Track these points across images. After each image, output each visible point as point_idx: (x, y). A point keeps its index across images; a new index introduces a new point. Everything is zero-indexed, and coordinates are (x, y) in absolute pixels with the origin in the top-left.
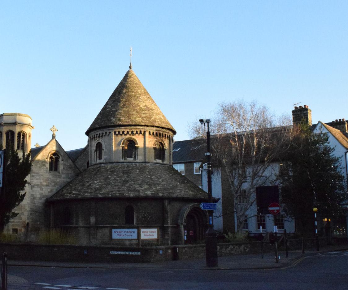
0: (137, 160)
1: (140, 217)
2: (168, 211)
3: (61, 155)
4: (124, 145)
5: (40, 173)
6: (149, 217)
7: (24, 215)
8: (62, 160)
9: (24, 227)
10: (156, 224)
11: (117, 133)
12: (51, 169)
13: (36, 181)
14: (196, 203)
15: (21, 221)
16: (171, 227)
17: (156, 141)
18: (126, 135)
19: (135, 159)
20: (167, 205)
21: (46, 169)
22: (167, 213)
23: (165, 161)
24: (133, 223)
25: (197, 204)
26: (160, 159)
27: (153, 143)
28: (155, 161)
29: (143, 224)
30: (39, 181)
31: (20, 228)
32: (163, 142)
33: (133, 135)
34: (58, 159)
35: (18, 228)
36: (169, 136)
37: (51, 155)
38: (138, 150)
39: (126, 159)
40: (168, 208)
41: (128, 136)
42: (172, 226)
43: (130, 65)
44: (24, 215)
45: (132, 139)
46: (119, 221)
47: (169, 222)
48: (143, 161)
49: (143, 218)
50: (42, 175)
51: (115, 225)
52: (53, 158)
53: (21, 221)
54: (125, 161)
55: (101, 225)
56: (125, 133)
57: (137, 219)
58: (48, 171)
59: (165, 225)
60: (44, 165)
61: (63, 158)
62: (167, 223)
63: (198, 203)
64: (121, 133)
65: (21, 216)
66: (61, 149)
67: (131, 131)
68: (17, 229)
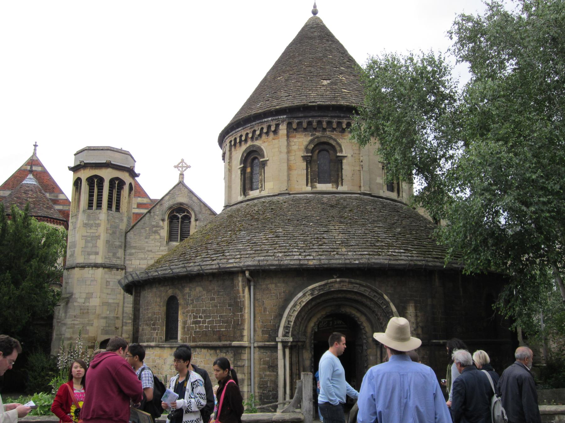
0: (264, 193)
1: (189, 322)
2: (244, 305)
3: (193, 210)
4: (242, 166)
5: (146, 249)
6: (204, 322)
7: (92, 325)
8: (196, 220)
10: (220, 340)
11: (233, 143)
12: (171, 237)
13: (137, 262)
14: (338, 280)
16: (260, 347)
17: (311, 142)
18: (246, 141)
19: (262, 190)
20: (241, 289)
21: (160, 239)
22: (241, 309)
23: (342, 185)
24: (177, 338)
25: (340, 282)
26: (330, 183)
27: (303, 147)
28: (309, 189)
29: (194, 341)
30: (145, 261)
32: (335, 140)
33: (257, 139)
34: (190, 218)
37: (172, 212)
38: (266, 168)
39: (249, 195)
40: (244, 297)
41: (250, 143)
42: (261, 344)
43: (315, 6)
44: (92, 325)
45: (254, 149)
46: (157, 335)
47: (245, 333)
48: (277, 192)
49: (194, 325)
50: (151, 251)
51: (153, 344)
52: (178, 218)
56: (243, 138)
57: (184, 328)
58: (165, 243)
59: (235, 343)
60: (156, 232)
61: (200, 216)
62: (241, 338)
63: (347, 280)
64: (238, 140)
65: (88, 328)
66: (194, 198)
67: (253, 130)
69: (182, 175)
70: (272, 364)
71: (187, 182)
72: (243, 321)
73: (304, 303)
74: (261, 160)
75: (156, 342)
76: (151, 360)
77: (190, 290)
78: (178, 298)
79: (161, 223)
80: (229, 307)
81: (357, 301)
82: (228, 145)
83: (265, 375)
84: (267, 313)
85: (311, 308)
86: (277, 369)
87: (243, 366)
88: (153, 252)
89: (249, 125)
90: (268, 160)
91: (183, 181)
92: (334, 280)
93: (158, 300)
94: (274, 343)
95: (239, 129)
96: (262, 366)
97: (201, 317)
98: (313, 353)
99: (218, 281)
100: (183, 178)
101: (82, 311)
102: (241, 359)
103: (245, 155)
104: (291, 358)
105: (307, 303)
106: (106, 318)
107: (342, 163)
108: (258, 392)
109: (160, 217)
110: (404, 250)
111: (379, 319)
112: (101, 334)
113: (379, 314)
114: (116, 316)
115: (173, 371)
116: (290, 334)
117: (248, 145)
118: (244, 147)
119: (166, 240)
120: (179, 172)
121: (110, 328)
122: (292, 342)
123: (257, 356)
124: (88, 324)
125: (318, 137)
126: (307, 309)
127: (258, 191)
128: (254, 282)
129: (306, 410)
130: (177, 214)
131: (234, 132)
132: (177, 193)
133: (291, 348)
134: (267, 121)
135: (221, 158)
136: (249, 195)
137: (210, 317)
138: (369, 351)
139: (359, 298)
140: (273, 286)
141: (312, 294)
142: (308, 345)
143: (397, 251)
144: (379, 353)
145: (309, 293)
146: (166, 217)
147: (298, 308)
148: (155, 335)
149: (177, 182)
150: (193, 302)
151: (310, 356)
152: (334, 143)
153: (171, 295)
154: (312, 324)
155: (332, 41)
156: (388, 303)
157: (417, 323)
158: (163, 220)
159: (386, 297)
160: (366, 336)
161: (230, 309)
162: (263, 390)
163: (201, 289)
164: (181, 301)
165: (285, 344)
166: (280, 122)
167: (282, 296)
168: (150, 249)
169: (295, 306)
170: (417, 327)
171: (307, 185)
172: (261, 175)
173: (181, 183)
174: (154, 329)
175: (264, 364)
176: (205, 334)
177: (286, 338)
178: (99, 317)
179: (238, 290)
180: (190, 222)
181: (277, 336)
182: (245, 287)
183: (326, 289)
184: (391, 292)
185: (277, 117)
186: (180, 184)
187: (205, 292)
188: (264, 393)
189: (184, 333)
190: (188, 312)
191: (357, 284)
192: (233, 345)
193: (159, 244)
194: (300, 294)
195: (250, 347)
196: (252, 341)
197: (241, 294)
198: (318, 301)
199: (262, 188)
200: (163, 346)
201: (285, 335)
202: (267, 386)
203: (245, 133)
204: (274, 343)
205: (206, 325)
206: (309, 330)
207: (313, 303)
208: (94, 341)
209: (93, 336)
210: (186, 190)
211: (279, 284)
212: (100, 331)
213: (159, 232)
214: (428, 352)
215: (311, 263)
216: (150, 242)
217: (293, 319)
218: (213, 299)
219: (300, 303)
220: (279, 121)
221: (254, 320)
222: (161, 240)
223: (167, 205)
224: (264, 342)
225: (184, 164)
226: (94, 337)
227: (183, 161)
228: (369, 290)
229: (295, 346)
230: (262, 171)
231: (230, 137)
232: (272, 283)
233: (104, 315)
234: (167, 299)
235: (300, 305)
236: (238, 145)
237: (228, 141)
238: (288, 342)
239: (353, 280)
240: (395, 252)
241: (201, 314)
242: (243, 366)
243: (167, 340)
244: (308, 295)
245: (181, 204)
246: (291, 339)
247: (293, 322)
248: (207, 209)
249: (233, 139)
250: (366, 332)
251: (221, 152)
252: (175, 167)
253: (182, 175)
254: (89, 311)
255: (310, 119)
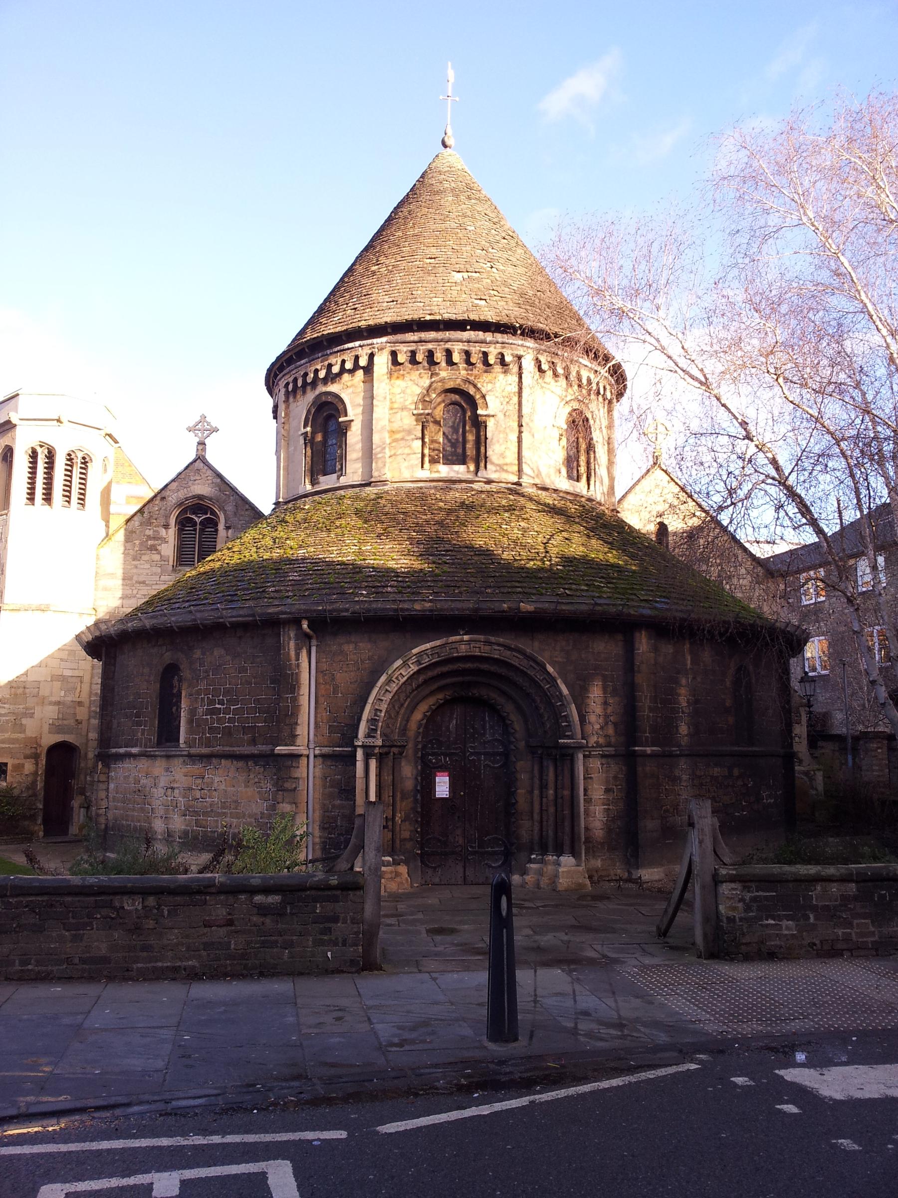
0: (343, 481)
1: (200, 710)
2: (298, 680)
7: (32, 716)
8: (228, 528)
9: (36, 757)
10: (254, 742)
11: (290, 387)
14: (466, 637)
15: (22, 736)
16: (323, 756)
19: (342, 475)
20: (293, 653)
22: (293, 686)
23: (486, 468)
28: (425, 474)
31: (16, 762)
32: (475, 386)
34: (216, 524)
35: (10, 762)
36: (508, 359)
37: (184, 511)
39: (318, 483)
40: (298, 666)
42: (326, 750)
44: (32, 716)
46: (143, 734)
49: (209, 717)
50: (144, 582)
51: (134, 750)
52: (195, 524)
53: (22, 736)
54: (318, 488)
55: (114, 750)
57: (190, 722)
58: (171, 568)
59: (280, 749)
60: (153, 548)
62: (292, 738)
63: (482, 637)
64: (300, 383)
65: (24, 721)
67: (326, 363)
68: (6, 764)
69: (202, 444)
70: (345, 786)
71: (210, 457)
72: (296, 708)
73: (405, 678)
74: (341, 420)
75: (141, 747)
76: (131, 780)
77: (203, 654)
78: (182, 667)
79: (163, 532)
80: (271, 684)
81: (500, 677)
82: (283, 391)
83: (334, 806)
84: (340, 695)
85: (418, 687)
86: (355, 796)
87: (295, 788)
88: (147, 585)
89: (320, 355)
90: (352, 421)
91: (204, 457)
92: (458, 637)
93: (146, 670)
94: (350, 749)
95: (303, 362)
96: (327, 790)
97: (221, 702)
98: (419, 767)
99: (253, 638)
100: (204, 450)
101: (13, 690)
102: (290, 778)
103: (313, 411)
104: (379, 775)
105: (411, 677)
106: (58, 703)
107: (486, 427)
108: (320, 837)
109: (162, 521)
110: (587, 585)
111: (537, 708)
112: (50, 733)
113: (538, 699)
114: (78, 700)
115: (170, 799)
116: (379, 732)
117: (317, 392)
118: (311, 396)
119: (171, 563)
120: (198, 440)
121: (65, 722)
122: (380, 747)
123: (318, 772)
124: (25, 715)
125: (442, 380)
126: (409, 688)
127: (335, 476)
128: (317, 638)
129: (370, 868)
130: (193, 516)
131: (293, 366)
132: (192, 478)
133: (381, 759)
134: (352, 348)
135: (272, 415)
136: (318, 483)
137: (236, 702)
138: (520, 765)
139: (503, 671)
140: (351, 647)
141: (418, 662)
142: (410, 750)
143: (574, 586)
144: (536, 768)
145: (414, 659)
146: (172, 521)
147: (394, 688)
148: (139, 734)
149: (193, 456)
150: (209, 676)
151: (415, 772)
152: (472, 391)
153: (169, 662)
154: (418, 716)
155: (478, 199)
156: (554, 680)
157: (606, 716)
158: (166, 526)
159: (550, 669)
160: (514, 738)
161: (275, 687)
162: (330, 833)
163: (223, 652)
164: (186, 673)
165: (369, 751)
166: (376, 350)
167: (367, 666)
168: (141, 579)
169: (389, 681)
170: (606, 724)
171: (422, 467)
172: (341, 447)
173: (200, 458)
174: (139, 724)
175: (331, 786)
176: (228, 732)
177: (370, 740)
178: (43, 701)
179: (289, 653)
180: (217, 531)
181: (356, 737)
182: (301, 649)
183: (444, 655)
184: (560, 660)
185: (369, 341)
186: (199, 460)
187: (228, 658)
188: (330, 838)
189: (190, 731)
190: (199, 693)
191: (499, 645)
192: (276, 752)
193: (159, 570)
194: (399, 662)
195: (308, 756)
196: (312, 746)
197: (294, 662)
198: (430, 674)
199: (341, 472)
200: (152, 753)
201: (368, 736)
202: (337, 826)
203: (313, 369)
204: (350, 749)
205: (231, 716)
206: (413, 725)
207: (421, 679)
208: (35, 746)
209: (34, 736)
210: (209, 472)
211: (361, 644)
212: (46, 728)
213: (159, 548)
214: (624, 768)
215: (417, 607)
216: (142, 567)
217: (384, 707)
218: (243, 670)
219: (397, 678)
220: (374, 348)
221: (316, 708)
222: (163, 563)
223: (173, 498)
224: (333, 747)
225: (205, 424)
226: (36, 737)
227: (204, 417)
228: (521, 657)
229: (387, 754)
230: (342, 441)
231: (286, 377)
232: (348, 643)
233: (54, 699)
234: (161, 670)
235: (396, 681)
236: (299, 392)
237: (282, 384)
238: (375, 747)
239: (493, 639)
240: (570, 589)
241: (221, 697)
242: (295, 788)
243: (159, 744)
244: (412, 664)
245: (200, 497)
246: (379, 742)
247: (384, 711)
248: (247, 507)
249: (291, 379)
250: (515, 730)
251: (269, 402)
252: (189, 430)
253: (202, 444)
254: (27, 691)
255: (430, 346)
